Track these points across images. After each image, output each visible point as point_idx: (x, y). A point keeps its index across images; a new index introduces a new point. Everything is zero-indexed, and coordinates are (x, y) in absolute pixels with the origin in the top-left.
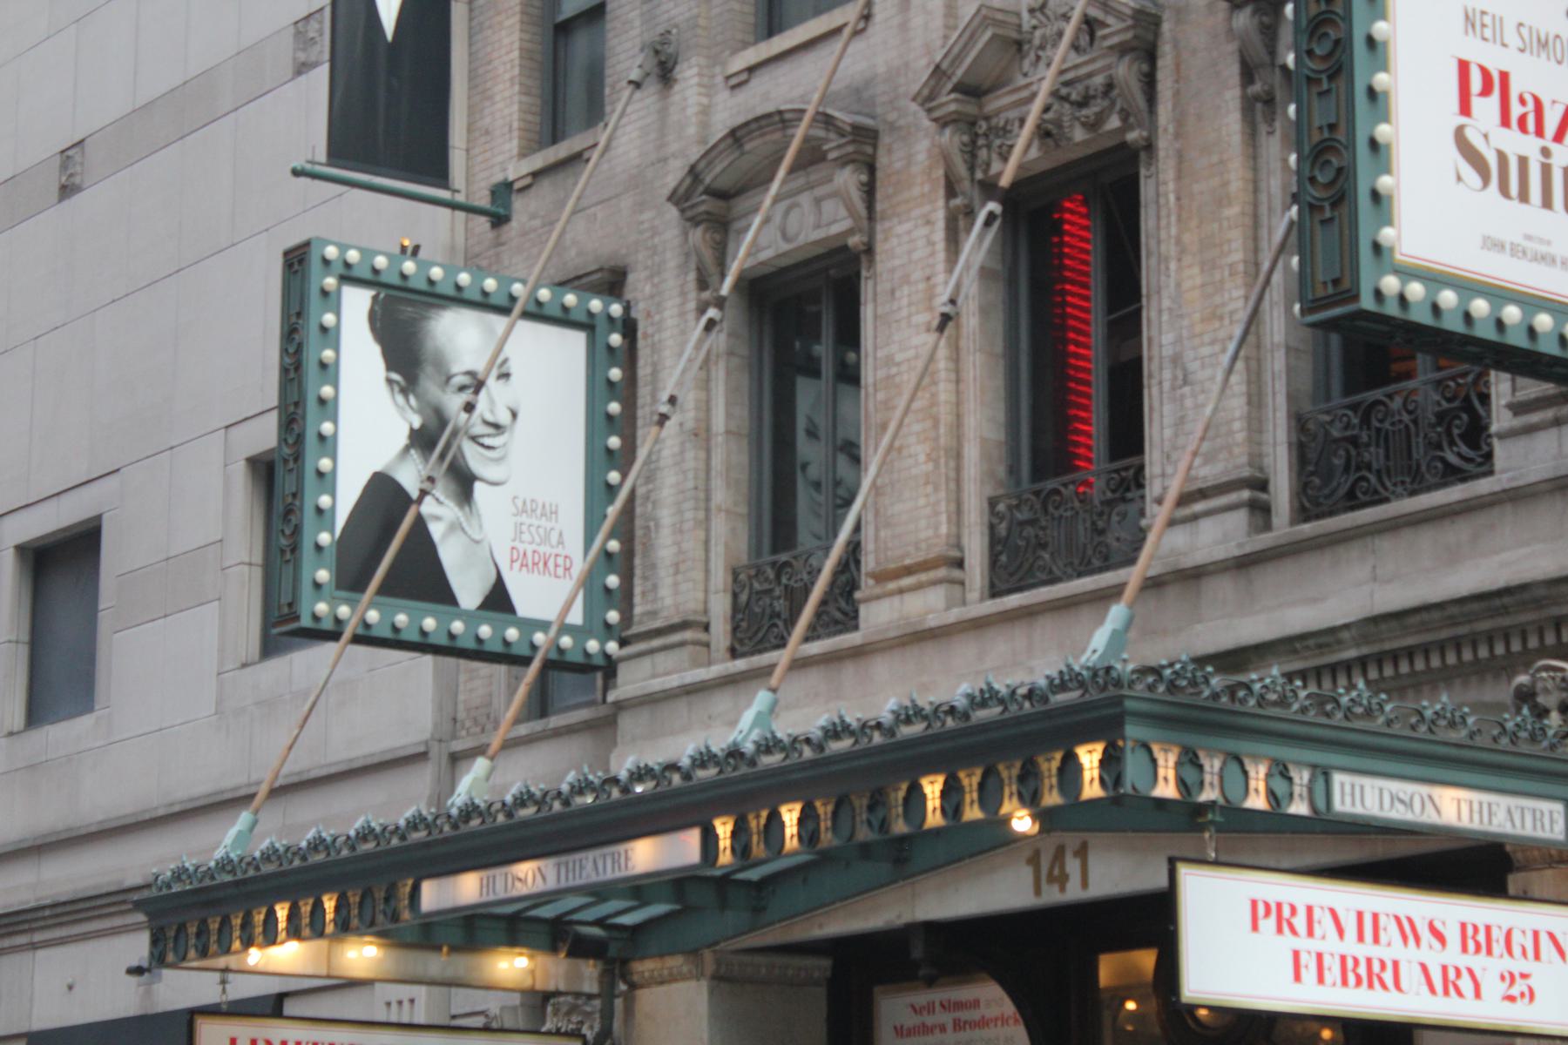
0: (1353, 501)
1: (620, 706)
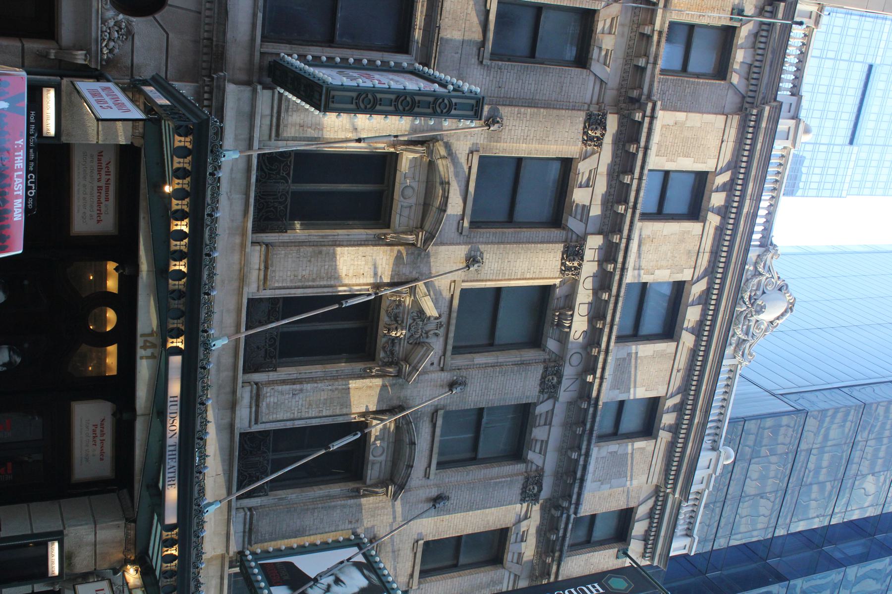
1: (254, 91)
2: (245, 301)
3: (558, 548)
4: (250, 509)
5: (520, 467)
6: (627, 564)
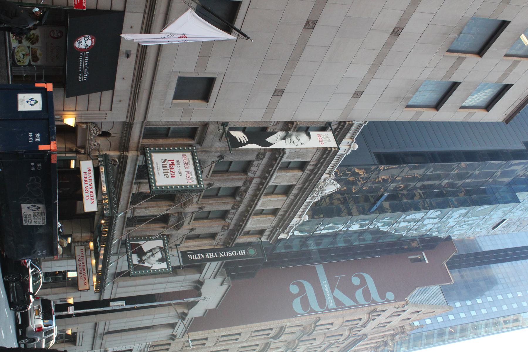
2: (131, 195)
5: (223, 222)
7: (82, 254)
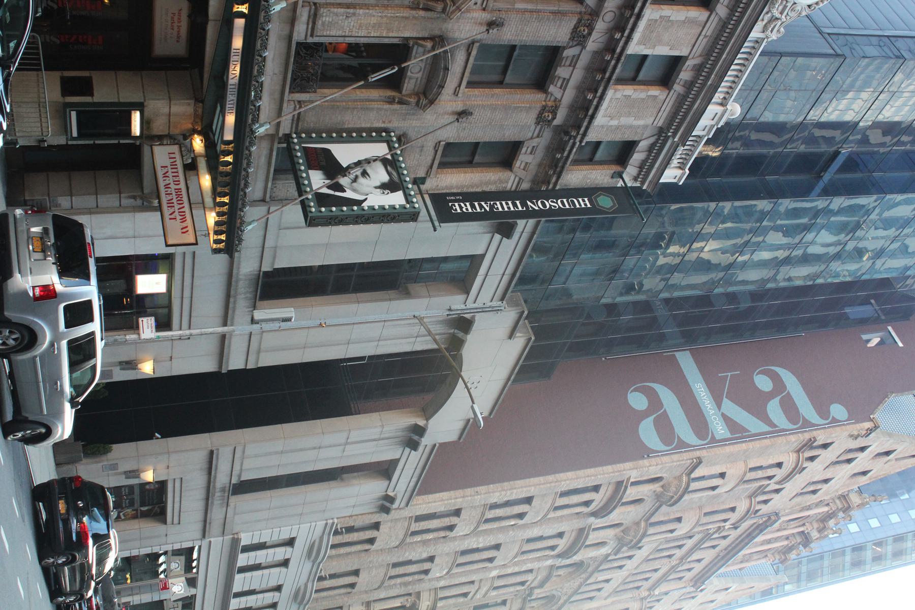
0: (297, 53)
3: (560, 165)
4: (299, 102)
5: (540, 96)
6: (619, 185)
7: (173, 164)
